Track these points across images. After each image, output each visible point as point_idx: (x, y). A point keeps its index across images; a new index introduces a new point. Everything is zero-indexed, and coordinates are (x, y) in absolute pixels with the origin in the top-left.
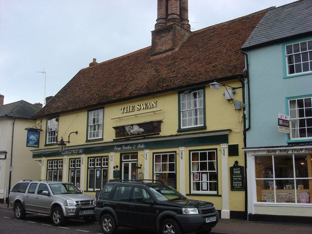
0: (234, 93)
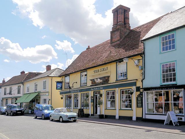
0: (139, 62)
